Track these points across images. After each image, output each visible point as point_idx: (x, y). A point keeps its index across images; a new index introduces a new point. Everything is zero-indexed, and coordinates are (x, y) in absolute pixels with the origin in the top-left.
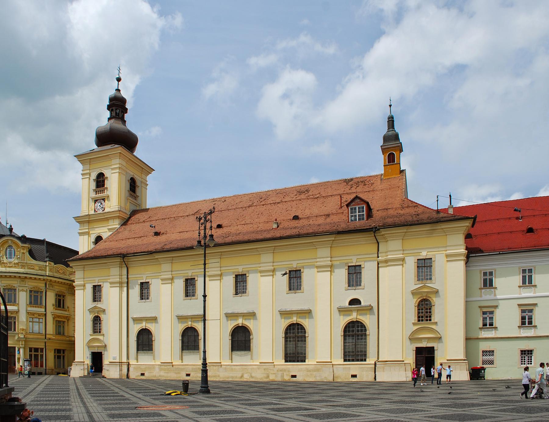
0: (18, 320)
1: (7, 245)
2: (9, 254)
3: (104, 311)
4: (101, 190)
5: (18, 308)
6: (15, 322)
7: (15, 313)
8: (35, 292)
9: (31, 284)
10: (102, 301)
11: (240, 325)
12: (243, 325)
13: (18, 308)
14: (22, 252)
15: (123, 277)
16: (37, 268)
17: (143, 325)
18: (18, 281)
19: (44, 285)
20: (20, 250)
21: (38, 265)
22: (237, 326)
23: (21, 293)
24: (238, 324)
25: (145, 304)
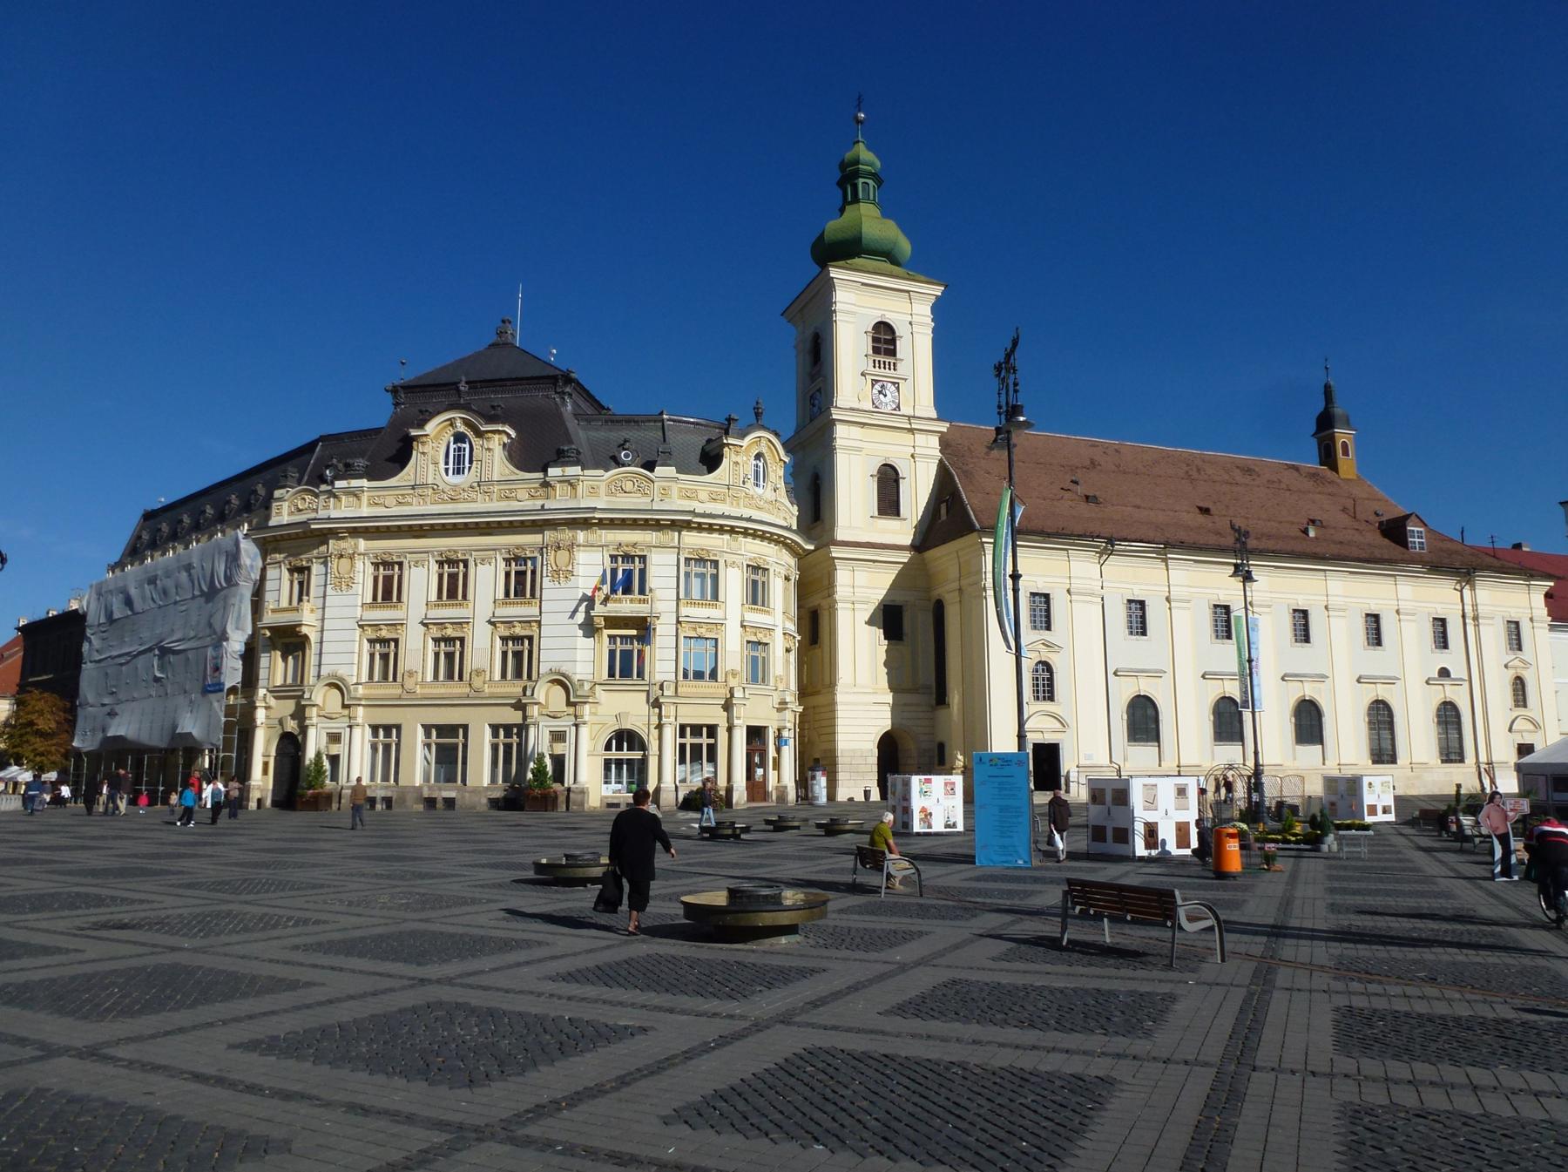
4: (882, 360)
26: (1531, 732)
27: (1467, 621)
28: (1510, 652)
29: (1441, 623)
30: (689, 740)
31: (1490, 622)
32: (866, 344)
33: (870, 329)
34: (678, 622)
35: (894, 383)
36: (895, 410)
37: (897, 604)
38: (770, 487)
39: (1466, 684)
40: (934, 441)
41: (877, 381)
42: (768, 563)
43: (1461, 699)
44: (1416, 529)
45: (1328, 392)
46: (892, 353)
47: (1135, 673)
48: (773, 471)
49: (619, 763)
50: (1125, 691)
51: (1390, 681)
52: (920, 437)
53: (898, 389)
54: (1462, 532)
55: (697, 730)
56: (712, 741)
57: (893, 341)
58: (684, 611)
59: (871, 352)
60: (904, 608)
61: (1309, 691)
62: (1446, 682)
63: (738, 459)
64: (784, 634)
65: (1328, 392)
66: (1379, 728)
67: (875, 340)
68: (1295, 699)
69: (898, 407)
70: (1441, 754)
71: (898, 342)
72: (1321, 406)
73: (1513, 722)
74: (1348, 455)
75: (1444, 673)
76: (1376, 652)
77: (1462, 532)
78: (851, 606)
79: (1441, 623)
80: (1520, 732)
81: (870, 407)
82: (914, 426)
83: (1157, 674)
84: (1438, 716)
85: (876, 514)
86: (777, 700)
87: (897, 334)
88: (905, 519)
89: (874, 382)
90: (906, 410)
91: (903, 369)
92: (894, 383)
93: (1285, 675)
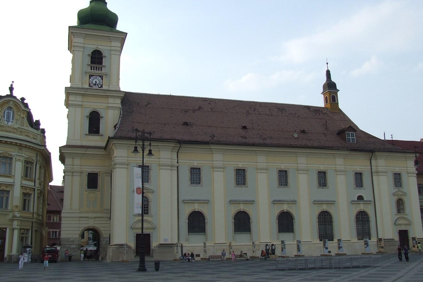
1: (7, 106)
2: (10, 117)
3: (153, 192)
4: (95, 66)
5: (14, 181)
7: (11, 186)
9: (27, 154)
10: (149, 181)
11: (285, 211)
12: (287, 211)
13: (14, 181)
14: (23, 116)
15: (173, 161)
16: (32, 136)
17: (197, 207)
18: (16, 149)
19: (35, 155)
20: (20, 114)
21: (32, 133)
22: (282, 211)
23: (17, 162)
24: (283, 210)
25: (196, 188)
26: (406, 225)
27: (373, 174)
28: (397, 188)
29: (359, 176)
31: (385, 174)
32: (88, 60)
33: (90, 54)
36: (100, 87)
37: (95, 173)
38: (14, 121)
39: (373, 203)
40: (119, 101)
42: (11, 155)
43: (370, 210)
44: (350, 133)
45: (328, 73)
46: (101, 63)
47: (192, 202)
48: (18, 115)
50: (187, 210)
51: (332, 203)
52: (111, 100)
54: (384, 134)
59: (90, 63)
60: (98, 174)
61: (285, 208)
62: (361, 202)
64: (22, 187)
65: (328, 73)
66: (325, 225)
67: (92, 58)
68: (278, 212)
69: (102, 86)
70: (358, 234)
71: (104, 59)
72: (324, 80)
73: (396, 220)
74: (335, 102)
75: (360, 198)
76: (323, 190)
77: (384, 134)
78: (71, 174)
79: (359, 176)
80: (400, 225)
81: (87, 86)
82: (107, 94)
83: (207, 202)
84: (356, 218)
85: (87, 133)
86: (11, 216)
87: (104, 55)
88: (102, 135)
89: (90, 76)
90: (104, 87)
91: (104, 71)
92: (100, 76)
93: (274, 201)
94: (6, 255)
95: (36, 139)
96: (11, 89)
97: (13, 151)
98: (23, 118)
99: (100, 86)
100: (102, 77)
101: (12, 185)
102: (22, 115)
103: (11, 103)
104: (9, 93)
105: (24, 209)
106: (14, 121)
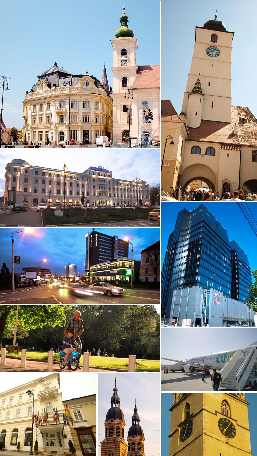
0: (91, 116)
6: (88, 118)
8: (96, 103)
30: (72, 133)
34: (70, 113)
35: (126, 61)
41: (122, 61)
49: (62, 137)
52: (131, 71)
53: (127, 62)
55: (74, 131)
56: (76, 133)
57: (126, 52)
58: (71, 110)
63: (81, 82)
67: (122, 53)
71: (127, 53)
81: (120, 66)
90: (128, 65)
92: (126, 61)
94: (89, 141)
95: (99, 92)
96: (87, 73)
97: (89, 98)
98: (93, 84)
99: (126, 65)
100: (127, 61)
101: (90, 113)
102: (92, 83)
103: (87, 78)
104: (86, 74)
105: (96, 122)
106: (89, 85)
